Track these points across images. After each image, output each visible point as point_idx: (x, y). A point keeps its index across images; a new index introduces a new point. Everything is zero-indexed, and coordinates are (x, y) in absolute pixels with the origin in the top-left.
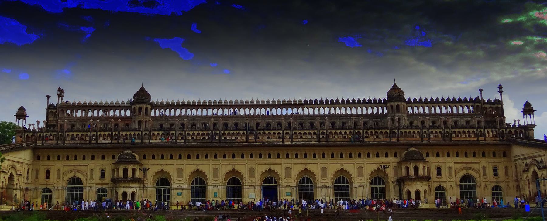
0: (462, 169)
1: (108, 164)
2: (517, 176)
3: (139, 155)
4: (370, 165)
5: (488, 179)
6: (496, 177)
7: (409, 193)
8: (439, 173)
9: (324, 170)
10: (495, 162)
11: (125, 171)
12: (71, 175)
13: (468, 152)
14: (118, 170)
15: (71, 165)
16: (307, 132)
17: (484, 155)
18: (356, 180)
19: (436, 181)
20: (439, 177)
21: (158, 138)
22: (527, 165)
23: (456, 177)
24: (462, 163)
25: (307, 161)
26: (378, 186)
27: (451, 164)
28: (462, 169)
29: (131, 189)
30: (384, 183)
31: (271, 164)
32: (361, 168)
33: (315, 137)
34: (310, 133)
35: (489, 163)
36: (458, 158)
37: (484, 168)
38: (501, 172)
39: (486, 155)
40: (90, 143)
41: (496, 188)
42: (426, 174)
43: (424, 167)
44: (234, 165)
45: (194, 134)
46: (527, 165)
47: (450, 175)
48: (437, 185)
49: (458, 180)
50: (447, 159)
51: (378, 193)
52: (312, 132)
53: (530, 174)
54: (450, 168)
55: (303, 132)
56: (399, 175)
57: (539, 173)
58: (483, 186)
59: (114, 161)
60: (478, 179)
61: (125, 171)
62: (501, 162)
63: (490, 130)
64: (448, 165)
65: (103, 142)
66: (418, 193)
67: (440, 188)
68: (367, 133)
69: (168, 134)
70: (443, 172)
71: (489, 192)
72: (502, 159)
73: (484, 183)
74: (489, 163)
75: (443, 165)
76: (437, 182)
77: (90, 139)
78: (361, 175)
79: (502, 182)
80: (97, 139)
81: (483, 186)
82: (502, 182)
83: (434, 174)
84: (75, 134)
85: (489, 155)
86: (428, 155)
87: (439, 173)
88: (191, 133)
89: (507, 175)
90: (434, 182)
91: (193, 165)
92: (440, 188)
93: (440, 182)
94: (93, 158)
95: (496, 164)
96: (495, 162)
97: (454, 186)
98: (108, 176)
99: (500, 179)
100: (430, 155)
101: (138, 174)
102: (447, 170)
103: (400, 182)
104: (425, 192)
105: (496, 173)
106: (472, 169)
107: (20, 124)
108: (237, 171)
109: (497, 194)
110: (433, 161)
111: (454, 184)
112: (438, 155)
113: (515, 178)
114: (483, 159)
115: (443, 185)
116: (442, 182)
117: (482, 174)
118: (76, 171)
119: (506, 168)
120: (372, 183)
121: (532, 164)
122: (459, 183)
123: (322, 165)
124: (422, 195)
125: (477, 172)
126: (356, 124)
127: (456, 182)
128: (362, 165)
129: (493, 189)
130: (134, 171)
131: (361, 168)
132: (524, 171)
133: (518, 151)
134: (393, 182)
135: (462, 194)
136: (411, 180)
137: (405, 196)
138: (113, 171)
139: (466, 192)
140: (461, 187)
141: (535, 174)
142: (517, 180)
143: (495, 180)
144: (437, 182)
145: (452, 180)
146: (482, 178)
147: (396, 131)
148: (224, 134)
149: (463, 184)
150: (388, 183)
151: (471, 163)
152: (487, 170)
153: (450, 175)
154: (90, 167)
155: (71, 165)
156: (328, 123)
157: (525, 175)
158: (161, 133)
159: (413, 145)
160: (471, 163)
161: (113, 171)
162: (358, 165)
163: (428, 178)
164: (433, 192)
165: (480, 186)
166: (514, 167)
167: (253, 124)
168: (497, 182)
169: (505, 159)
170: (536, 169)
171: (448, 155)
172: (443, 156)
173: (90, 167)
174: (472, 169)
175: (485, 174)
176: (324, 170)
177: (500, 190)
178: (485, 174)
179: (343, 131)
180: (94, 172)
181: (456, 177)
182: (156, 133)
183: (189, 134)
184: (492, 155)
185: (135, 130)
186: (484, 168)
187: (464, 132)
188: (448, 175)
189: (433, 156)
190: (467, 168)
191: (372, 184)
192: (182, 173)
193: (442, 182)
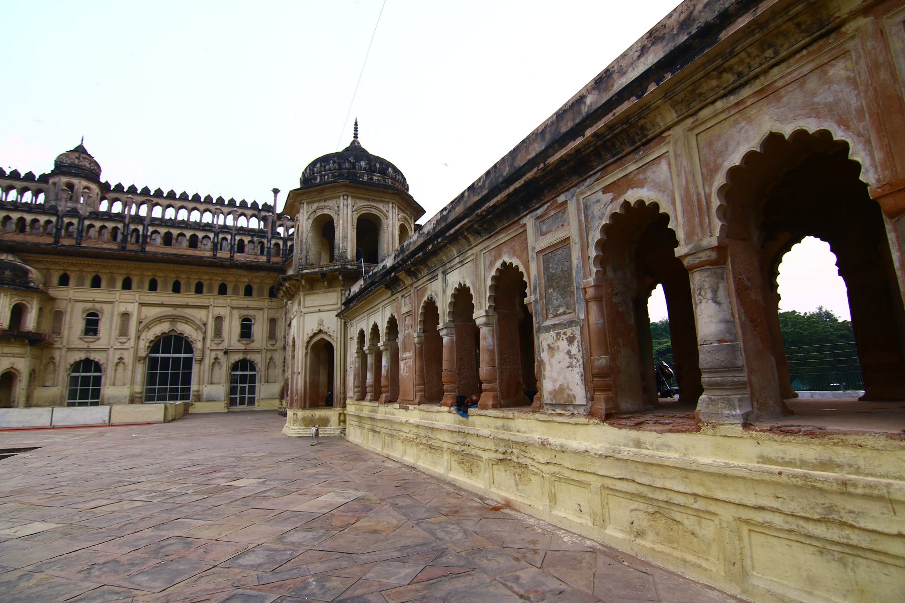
0: (159, 320)
5: (225, 345)
6: (245, 341)
8: (92, 325)
10: (247, 308)
13: (182, 282)
17: (223, 290)
20: (90, 338)
27: (132, 308)
28: (159, 320)
35: (233, 308)
36: (153, 293)
37: (219, 320)
38: (259, 330)
39: (230, 290)
41: (244, 364)
47: (124, 332)
48: (80, 356)
49: (143, 345)
50: (119, 295)
54: (126, 316)
58: (207, 362)
60: (199, 345)
62: (261, 309)
64: (122, 308)
67: (88, 364)
70: (103, 327)
71: (222, 373)
72: (266, 303)
73: (213, 355)
74: (233, 308)
79: (258, 351)
81: (207, 362)
82: (258, 351)
85: (236, 291)
89: (272, 336)
90: (70, 350)
92: (88, 364)
93: (88, 350)
95: (251, 313)
96: (247, 308)
99: (254, 346)
102: (117, 321)
105: (246, 331)
106: (187, 321)
109: (243, 379)
111: (129, 357)
114: (221, 300)
116: (95, 350)
117: (210, 333)
119: (273, 322)
122: (143, 353)
125: (198, 328)
127: (136, 351)
129: (235, 367)
135: (151, 379)
143: (242, 347)
145: (126, 346)
146: (208, 342)
151: (187, 306)
152: (226, 325)
153: (124, 332)
160: (187, 306)
165: (200, 361)
168: (245, 351)
169: (275, 303)
171: (127, 285)
172: (112, 284)
174: (187, 321)
175: (218, 333)
177: (253, 368)
178: (218, 333)
184: (242, 291)
186: (219, 320)
188: (115, 332)
190: (174, 319)
193: (95, 350)
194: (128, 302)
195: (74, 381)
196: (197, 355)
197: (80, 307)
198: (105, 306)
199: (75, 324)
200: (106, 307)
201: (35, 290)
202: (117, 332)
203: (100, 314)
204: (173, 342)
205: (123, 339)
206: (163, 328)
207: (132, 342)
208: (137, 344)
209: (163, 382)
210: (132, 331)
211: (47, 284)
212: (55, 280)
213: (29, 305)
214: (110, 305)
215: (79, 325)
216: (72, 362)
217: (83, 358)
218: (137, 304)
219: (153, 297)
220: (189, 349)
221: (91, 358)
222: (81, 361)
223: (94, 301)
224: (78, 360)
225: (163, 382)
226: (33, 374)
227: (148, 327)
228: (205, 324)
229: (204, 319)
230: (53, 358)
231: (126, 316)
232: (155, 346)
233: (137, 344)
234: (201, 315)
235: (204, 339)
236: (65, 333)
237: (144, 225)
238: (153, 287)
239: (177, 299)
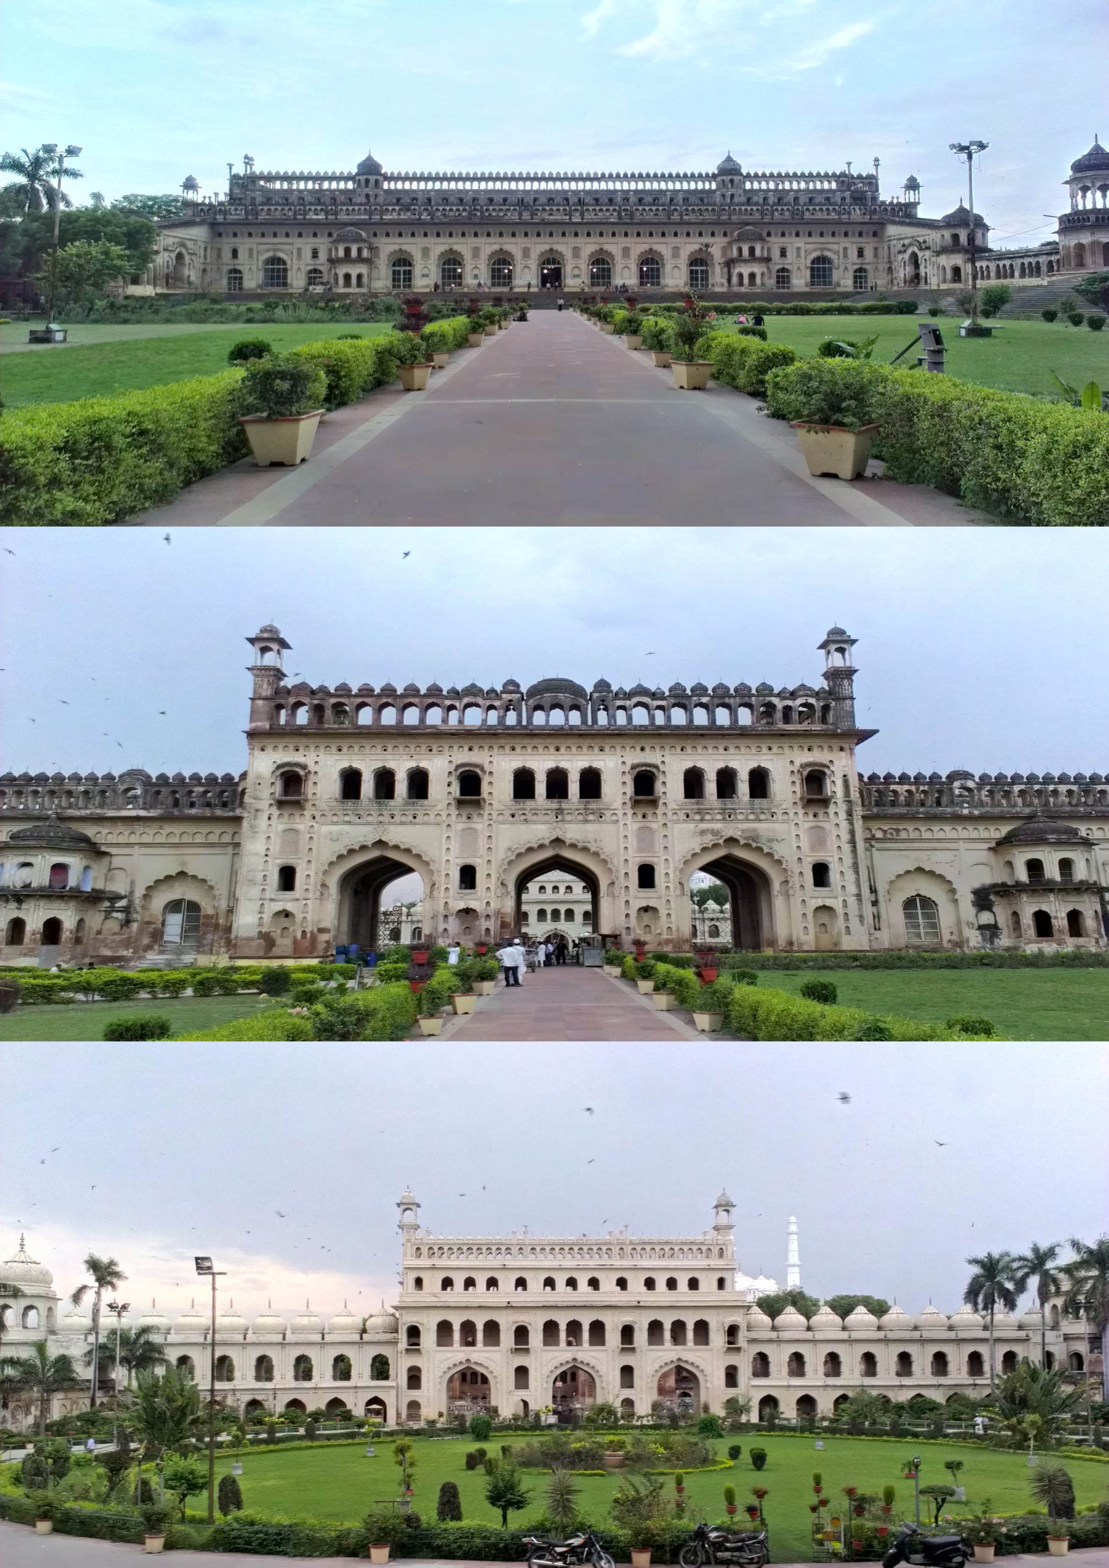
1: (323, 244)
2: (889, 257)
3: (368, 234)
7: (741, 276)
8: (783, 253)
11: (348, 251)
14: (337, 249)
16: (604, 208)
19: (777, 262)
21: (395, 214)
22: (904, 245)
27: (800, 245)
28: (815, 250)
29: (354, 271)
30: (707, 265)
33: (615, 214)
34: (608, 210)
40: (295, 219)
42: (766, 255)
43: (762, 248)
45: (444, 210)
46: (904, 245)
47: (798, 256)
52: (611, 208)
53: (907, 256)
54: (798, 249)
55: (598, 208)
56: (729, 256)
57: (920, 254)
59: (331, 239)
61: (348, 251)
63: (857, 208)
64: (797, 245)
65: (315, 217)
66: (752, 276)
68: (687, 210)
69: (408, 210)
70: (788, 254)
77: (295, 214)
80: (305, 213)
83: (776, 254)
84: (273, 208)
87: (783, 253)
88: (441, 208)
92: (783, 270)
94: (300, 235)
97: (802, 268)
98: (323, 256)
101: (365, 253)
102: (795, 251)
103: (729, 264)
104: (763, 274)
107: (190, 195)
113: (886, 260)
120: (691, 264)
121: (911, 245)
124: (758, 280)
126: (672, 200)
130: (360, 250)
132: (900, 252)
133: (892, 230)
136: (745, 261)
137: (735, 280)
138: (330, 250)
140: (812, 269)
141: (914, 256)
142: (890, 262)
148: (487, 210)
150: (713, 264)
153: (798, 256)
154: (296, 246)
156: (633, 199)
157: (900, 257)
158: (397, 208)
159: (748, 224)
161: (330, 250)
163: (768, 260)
164: (774, 275)
166: (886, 248)
167: (529, 199)
170: (916, 249)
173: (296, 246)
174: (829, 250)
179: (654, 208)
180: (303, 252)
182: (390, 208)
183: (437, 210)
185: (361, 204)
187: (821, 210)
188: (795, 255)
190: (822, 249)
194: (800, 242)
195: (778, 277)
204: (821, 260)
209: (499, 278)
210: (803, 254)
219: (811, 240)
231: (798, 249)
232: (813, 262)
234: (835, 247)
238: (810, 235)
239: (822, 240)
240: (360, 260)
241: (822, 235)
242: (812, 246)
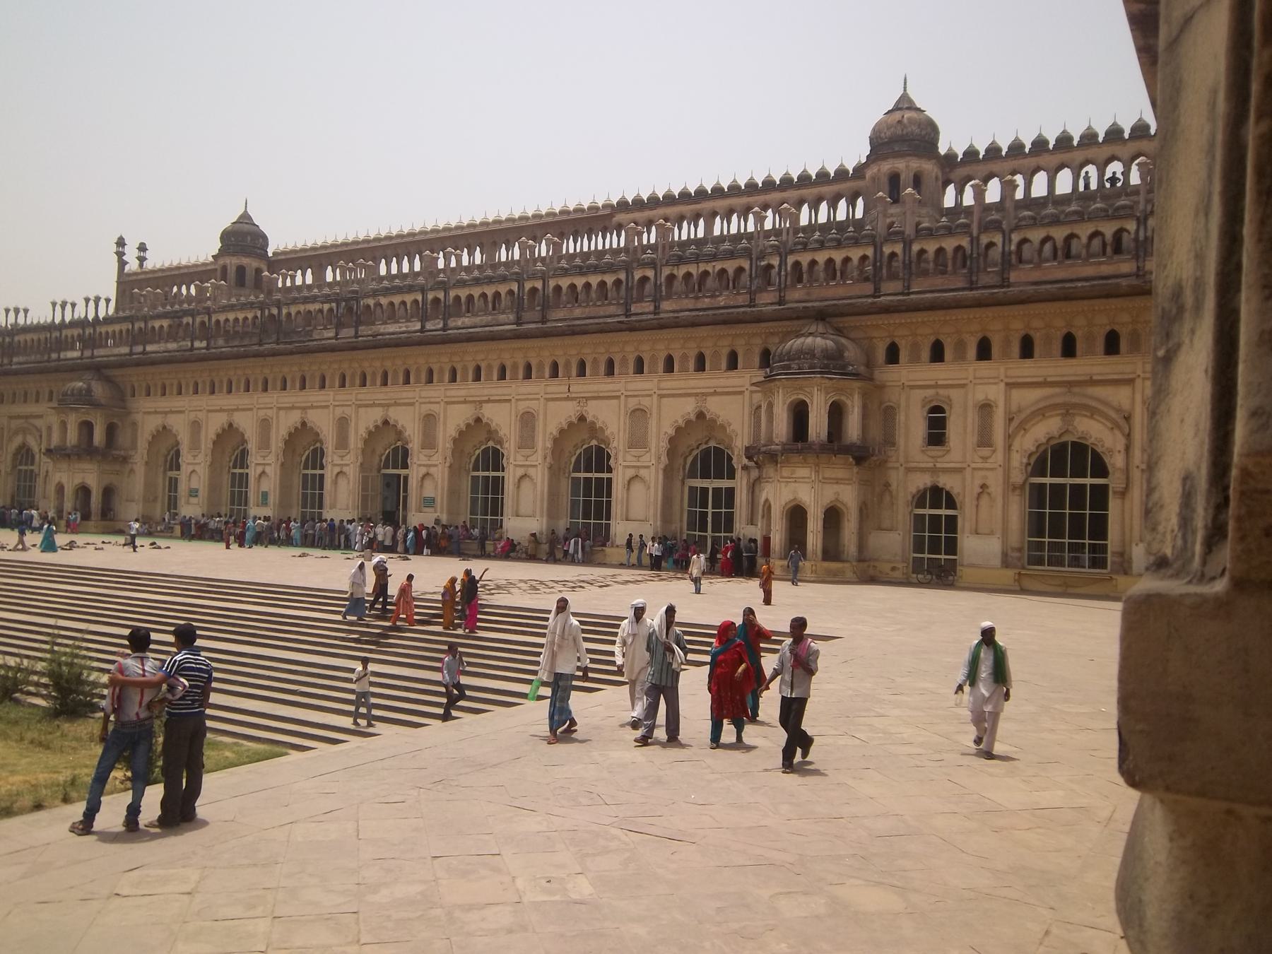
0: (1041, 413)
4: (670, 402)
9: (527, 421)
12: (18, 440)
15: (19, 417)
18: (620, 460)
20: (936, 451)
23: (1009, 448)
24: (1045, 384)
25: (581, 387)
26: (711, 484)
27: (995, 393)
28: (1041, 413)
31: (389, 405)
32: (639, 414)
44: (304, 409)
47: (985, 440)
51: (710, 510)
54: (986, 408)
64: (981, 393)
67: (937, 496)
70: (953, 430)
75: (955, 394)
76: (923, 470)
78: (637, 442)
86: (893, 355)
87: (937, 433)
91: (221, 410)
93: (934, 471)
97: (996, 487)
100: (903, 355)
102: (972, 418)
108: (312, 428)
110: (913, 384)
112: (937, 354)
115: (946, 482)
116: (946, 471)
118: (24, 431)
122: (1017, 477)
123: (523, 406)
125: (1115, 426)
128: (646, 402)
131: (639, 414)
134: (745, 468)
139: (1057, 519)
144: (923, 470)
147: (775, 262)
149: (1048, 480)
151: (1092, 382)
153: (985, 440)
155: (19, 417)
160: (1092, 382)
162: (633, 403)
174: (1092, 412)
176: (527, 421)
181: (1009, 448)
188: (972, 439)
189: (915, 359)
191: (692, 475)
192: (199, 432)
196: (1114, 482)
197: (918, 395)
198: (954, 394)
199: (914, 427)
200: (955, 394)
201: (856, 375)
202: (975, 439)
203: (946, 407)
205: (985, 451)
206: (1044, 430)
207: (999, 457)
208: (1008, 458)
211: (869, 364)
212: (881, 354)
213: (849, 402)
214: (962, 391)
215: (919, 429)
216: (914, 490)
217: (929, 485)
218: (1002, 385)
219: (1027, 369)
220: (1101, 469)
221: (940, 485)
222: (925, 490)
223: (936, 386)
224: (922, 487)
225: (1056, 532)
226: (864, 510)
227: (1022, 427)
228: (1128, 419)
229: (1126, 404)
230: (887, 485)
231: (986, 408)
233: (1008, 458)
234: (1121, 396)
235: (1128, 448)
236: (901, 441)
237: (1003, 232)
238: (1027, 349)
240: (85, 450)
241: (1069, 348)
242: (1030, 397)
